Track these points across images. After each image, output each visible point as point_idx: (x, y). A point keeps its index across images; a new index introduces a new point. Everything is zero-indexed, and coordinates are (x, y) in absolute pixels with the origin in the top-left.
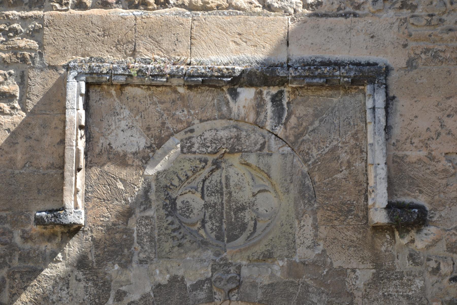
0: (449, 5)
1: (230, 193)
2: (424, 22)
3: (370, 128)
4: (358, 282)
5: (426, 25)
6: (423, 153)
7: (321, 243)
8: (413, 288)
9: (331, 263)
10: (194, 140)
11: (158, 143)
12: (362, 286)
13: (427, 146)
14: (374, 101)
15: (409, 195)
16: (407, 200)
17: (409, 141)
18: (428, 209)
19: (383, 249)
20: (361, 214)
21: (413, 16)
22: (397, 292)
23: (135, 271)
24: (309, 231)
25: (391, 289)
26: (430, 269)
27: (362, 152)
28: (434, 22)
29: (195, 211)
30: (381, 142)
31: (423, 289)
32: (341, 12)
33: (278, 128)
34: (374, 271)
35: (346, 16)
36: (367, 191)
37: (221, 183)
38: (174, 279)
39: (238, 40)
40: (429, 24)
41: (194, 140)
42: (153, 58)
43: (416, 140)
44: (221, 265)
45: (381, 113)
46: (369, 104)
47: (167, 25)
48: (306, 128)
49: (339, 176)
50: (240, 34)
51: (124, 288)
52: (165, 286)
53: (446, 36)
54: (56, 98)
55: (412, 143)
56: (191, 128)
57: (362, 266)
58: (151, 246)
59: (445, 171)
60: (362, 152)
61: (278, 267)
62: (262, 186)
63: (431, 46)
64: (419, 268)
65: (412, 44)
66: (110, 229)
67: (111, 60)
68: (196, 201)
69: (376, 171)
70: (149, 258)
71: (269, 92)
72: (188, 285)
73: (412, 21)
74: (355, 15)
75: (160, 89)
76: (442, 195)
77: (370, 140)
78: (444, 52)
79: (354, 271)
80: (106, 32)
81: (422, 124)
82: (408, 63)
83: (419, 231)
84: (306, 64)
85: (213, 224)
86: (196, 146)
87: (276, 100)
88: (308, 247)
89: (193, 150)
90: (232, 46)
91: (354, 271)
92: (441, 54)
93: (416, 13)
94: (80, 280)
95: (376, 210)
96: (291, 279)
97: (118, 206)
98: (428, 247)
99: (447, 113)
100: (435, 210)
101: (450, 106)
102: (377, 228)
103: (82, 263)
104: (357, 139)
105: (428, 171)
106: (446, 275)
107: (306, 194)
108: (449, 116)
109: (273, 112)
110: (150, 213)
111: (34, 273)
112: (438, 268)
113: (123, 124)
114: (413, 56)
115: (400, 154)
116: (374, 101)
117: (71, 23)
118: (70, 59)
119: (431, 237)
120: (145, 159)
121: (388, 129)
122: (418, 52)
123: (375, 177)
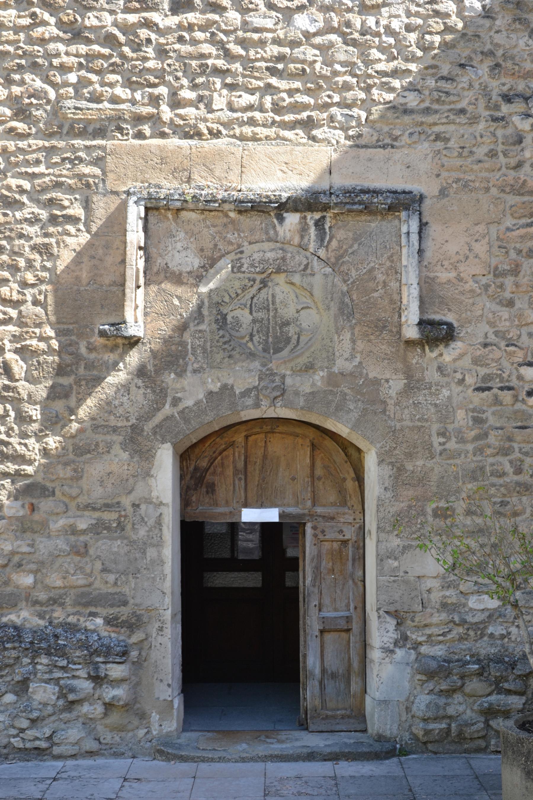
0: (479, 138)
1: (276, 309)
2: (456, 154)
3: (405, 251)
4: (391, 391)
5: (457, 157)
6: (452, 275)
7: (358, 355)
8: (441, 397)
9: (367, 374)
10: (243, 261)
11: (210, 263)
12: (394, 395)
13: (456, 268)
14: (409, 226)
15: (438, 313)
16: (437, 317)
17: (440, 263)
18: (455, 325)
19: (414, 361)
20: (394, 330)
21: (446, 148)
22: (426, 400)
23: (189, 380)
24: (347, 345)
25: (420, 398)
26: (456, 380)
27: (396, 273)
28: (465, 153)
29: (244, 326)
30: (414, 264)
31: (450, 398)
32: (380, 143)
33: (320, 250)
34: (406, 381)
35: (384, 147)
36: (400, 308)
37: (267, 300)
38: (224, 387)
39: (284, 168)
40: (460, 155)
41: (243, 261)
42: (207, 184)
43: (446, 263)
45: (414, 237)
46: (404, 229)
47: (220, 154)
48: (346, 251)
49: (376, 295)
50: (286, 163)
51: (179, 395)
52: (216, 393)
53: (475, 167)
54: (117, 222)
55: (442, 266)
56: (241, 249)
57: (394, 377)
58: (204, 357)
59: (472, 291)
60: (396, 273)
61: (319, 378)
62: (304, 303)
63: (462, 176)
64: (446, 379)
65: (444, 174)
66: (167, 341)
67: (168, 186)
68: (245, 317)
69: (409, 291)
70: (202, 367)
71: (312, 217)
72: (237, 392)
73: (444, 152)
74: (393, 147)
75: (213, 213)
76: (469, 313)
77: (404, 262)
78: (474, 181)
79: (387, 381)
80: (163, 160)
81: (452, 248)
82: (440, 191)
83: (447, 345)
84: (347, 192)
85: (260, 338)
86: (246, 266)
87: (319, 224)
88: (346, 359)
89: (243, 269)
90: (280, 174)
91: (387, 381)
92: (471, 184)
93: (448, 146)
94: (139, 388)
95: (409, 326)
96: (330, 388)
97: (174, 320)
98: (455, 360)
99: (475, 238)
100: (462, 326)
101: (478, 232)
102: (409, 343)
103: (141, 371)
104: (392, 261)
105: (456, 291)
106: (470, 386)
107: (346, 311)
108: (476, 241)
109: (316, 235)
110: (203, 327)
111: (99, 380)
112: (463, 380)
113: (179, 245)
114: (445, 185)
115: (432, 275)
116: (409, 226)
117: (131, 152)
118: (130, 185)
119: (458, 351)
120: (199, 278)
121: (420, 252)
122: (450, 181)
123: (408, 296)
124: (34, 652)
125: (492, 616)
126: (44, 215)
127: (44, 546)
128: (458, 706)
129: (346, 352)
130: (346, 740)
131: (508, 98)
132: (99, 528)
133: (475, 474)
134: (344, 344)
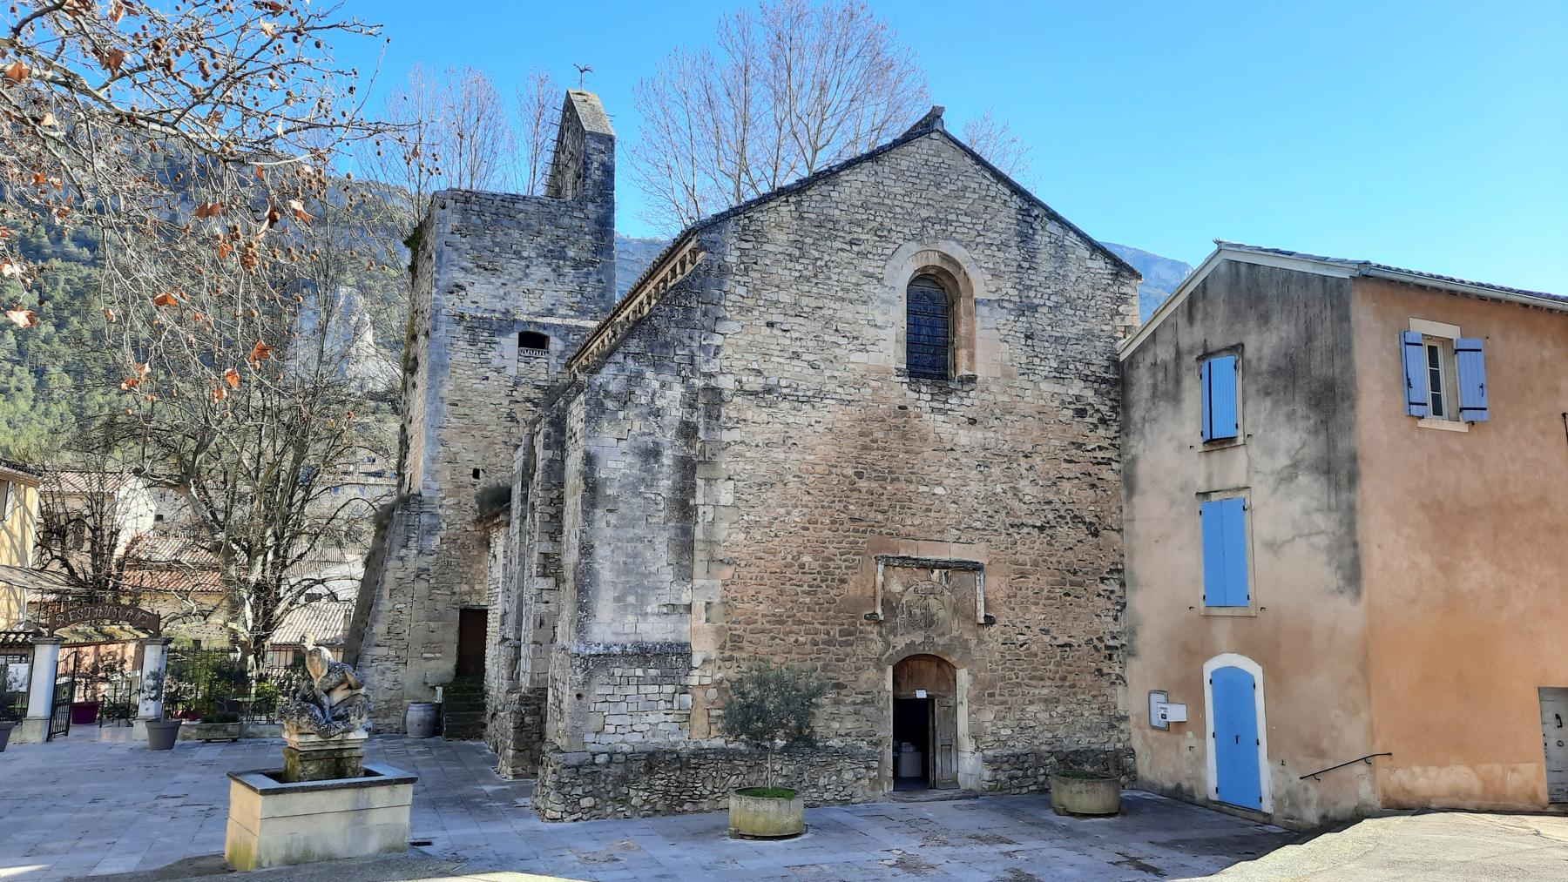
23: (899, 638)
68: (918, 611)
125: (1010, 737)
126: (843, 565)
127: (843, 709)
128: (1002, 776)
129: (957, 628)
130: (951, 793)
132: (864, 702)
133: (1003, 678)
134: (955, 625)
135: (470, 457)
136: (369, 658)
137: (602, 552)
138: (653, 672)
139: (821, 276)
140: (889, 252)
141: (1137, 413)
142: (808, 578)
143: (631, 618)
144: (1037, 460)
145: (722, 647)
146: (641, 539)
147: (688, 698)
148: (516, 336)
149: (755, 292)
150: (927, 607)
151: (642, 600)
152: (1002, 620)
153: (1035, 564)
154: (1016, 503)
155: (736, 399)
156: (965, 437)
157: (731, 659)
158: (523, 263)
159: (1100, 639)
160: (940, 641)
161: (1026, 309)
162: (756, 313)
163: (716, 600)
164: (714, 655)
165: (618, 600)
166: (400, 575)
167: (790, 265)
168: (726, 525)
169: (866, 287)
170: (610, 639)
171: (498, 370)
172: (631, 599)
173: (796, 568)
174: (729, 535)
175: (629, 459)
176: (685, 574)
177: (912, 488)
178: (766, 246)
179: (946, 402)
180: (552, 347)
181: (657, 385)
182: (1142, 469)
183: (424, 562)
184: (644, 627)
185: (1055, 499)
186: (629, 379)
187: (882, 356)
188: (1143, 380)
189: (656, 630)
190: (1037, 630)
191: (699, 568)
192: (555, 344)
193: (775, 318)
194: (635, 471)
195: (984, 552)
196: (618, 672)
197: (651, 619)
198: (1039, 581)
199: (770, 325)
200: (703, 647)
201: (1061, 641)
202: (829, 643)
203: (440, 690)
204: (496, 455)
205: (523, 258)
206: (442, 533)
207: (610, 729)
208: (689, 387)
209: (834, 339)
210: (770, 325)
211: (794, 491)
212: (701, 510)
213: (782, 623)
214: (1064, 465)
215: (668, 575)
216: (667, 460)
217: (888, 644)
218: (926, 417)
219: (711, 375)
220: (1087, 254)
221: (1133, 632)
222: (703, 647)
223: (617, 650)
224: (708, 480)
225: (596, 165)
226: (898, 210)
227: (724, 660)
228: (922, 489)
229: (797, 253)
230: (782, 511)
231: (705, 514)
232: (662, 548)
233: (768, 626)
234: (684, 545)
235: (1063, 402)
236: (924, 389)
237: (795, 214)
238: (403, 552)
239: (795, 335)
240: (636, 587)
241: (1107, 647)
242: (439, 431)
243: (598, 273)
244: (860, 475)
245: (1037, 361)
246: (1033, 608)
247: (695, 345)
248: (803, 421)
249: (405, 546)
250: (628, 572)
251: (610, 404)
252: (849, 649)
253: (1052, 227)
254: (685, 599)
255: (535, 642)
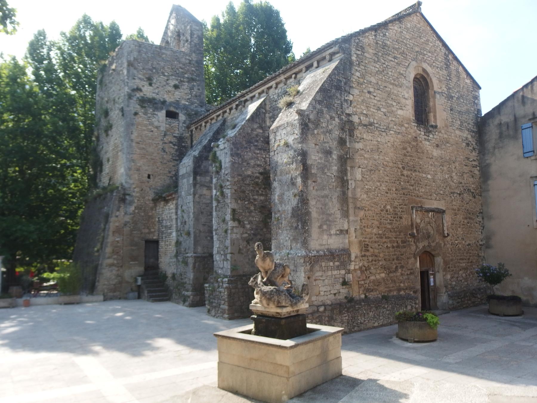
23: (421, 243)
44: (429, 243)
124: (407, 299)
125: (455, 285)
131: (451, 193)
132: (411, 273)
135: (146, 169)
136: (104, 265)
137: (312, 203)
138: (337, 264)
139: (385, 72)
140: (407, 64)
141: (490, 146)
142: (389, 216)
143: (325, 237)
144: (457, 164)
145: (361, 250)
146: (327, 196)
147: (350, 276)
148: (164, 112)
149: (363, 76)
150: (427, 230)
151: (329, 227)
152: (451, 234)
153: (459, 210)
154: (452, 183)
155: (360, 128)
156: (436, 153)
157: (365, 256)
158: (166, 78)
159: (478, 241)
160: (433, 244)
161: (450, 97)
162: (364, 86)
163: (358, 227)
164: (359, 254)
165: (320, 227)
166: (117, 224)
167: (375, 65)
168: (359, 190)
169: (400, 79)
170: (318, 248)
171: (157, 127)
172: (325, 227)
173: (385, 211)
174: (361, 195)
175: (320, 155)
176: (346, 214)
177: (421, 174)
178: (365, 54)
179: (428, 136)
180: (180, 118)
181: (328, 117)
182: (493, 169)
183: (127, 218)
184: (331, 241)
185: (463, 182)
186: (318, 113)
187: (408, 112)
188: (492, 131)
189: (334, 242)
190: (460, 238)
191: (351, 211)
192: (182, 117)
193: (372, 90)
194: (323, 161)
195: (444, 204)
196: (323, 264)
197: (334, 237)
198: (460, 217)
199: (369, 92)
200: (355, 251)
201: (467, 243)
202: (398, 247)
203: (139, 279)
204: (157, 168)
205: (165, 76)
206: (135, 205)
207: (322, 293)
208: (341, 120)
209: (391, 102)
210: (369, 92)
211: (382, 175)
212: (350, 182)
213: (381, 238)
214: (465, 167)
215: (338, 214)
216: (335, 157)
217: (417, 247)
218: (423, 142)
219: (349, 115)
220: (465, 76)
221: (488, 238)
222: (355, 251)
223: (321, 253)
224: (352, 167)
225: (195, 36)
226: (408, 46)
227: (362, 256)
228: (424, 175)
229: (376, 59)
230: (379, 184)
231: (352, 184)
232: (335, 201)
233: (377, 240)
234: (344, 199)
235: (462, 140)
236: (422, 129)
237: (375, 41)
238: (118, 213)
239: (378, 99)
240: (327, 222)
241: (480, 245)
242: (131, 156)
243: (198, 86)
244: (403, 168)
245: (454, 120)
246: (459, 229)
247: (343, 99)
248: (383, 141)
249: (118, 210)
250: (323, 213)
251: (311, 125)
252: (404, 250)
253: (455, 63)
254: (346, 227)
255: (231, 253)
